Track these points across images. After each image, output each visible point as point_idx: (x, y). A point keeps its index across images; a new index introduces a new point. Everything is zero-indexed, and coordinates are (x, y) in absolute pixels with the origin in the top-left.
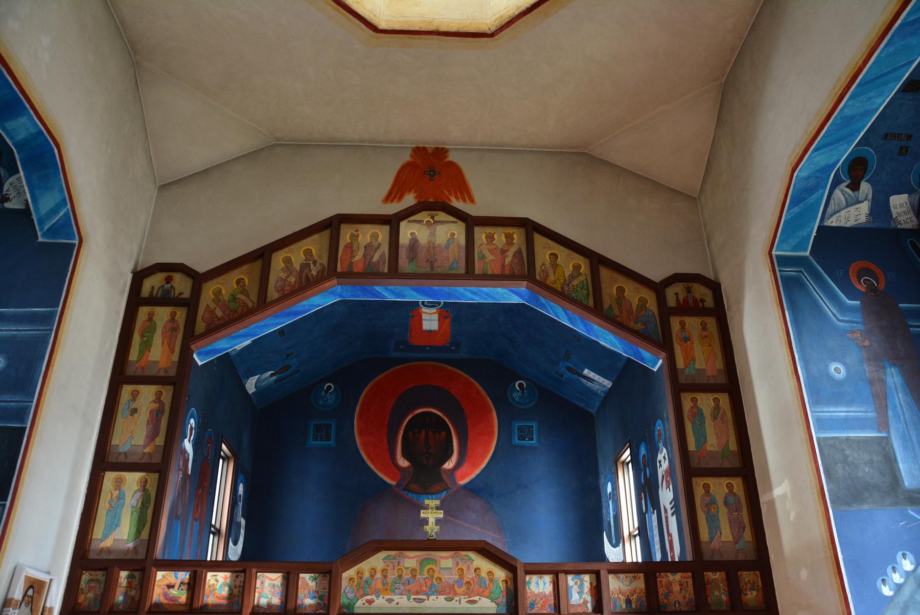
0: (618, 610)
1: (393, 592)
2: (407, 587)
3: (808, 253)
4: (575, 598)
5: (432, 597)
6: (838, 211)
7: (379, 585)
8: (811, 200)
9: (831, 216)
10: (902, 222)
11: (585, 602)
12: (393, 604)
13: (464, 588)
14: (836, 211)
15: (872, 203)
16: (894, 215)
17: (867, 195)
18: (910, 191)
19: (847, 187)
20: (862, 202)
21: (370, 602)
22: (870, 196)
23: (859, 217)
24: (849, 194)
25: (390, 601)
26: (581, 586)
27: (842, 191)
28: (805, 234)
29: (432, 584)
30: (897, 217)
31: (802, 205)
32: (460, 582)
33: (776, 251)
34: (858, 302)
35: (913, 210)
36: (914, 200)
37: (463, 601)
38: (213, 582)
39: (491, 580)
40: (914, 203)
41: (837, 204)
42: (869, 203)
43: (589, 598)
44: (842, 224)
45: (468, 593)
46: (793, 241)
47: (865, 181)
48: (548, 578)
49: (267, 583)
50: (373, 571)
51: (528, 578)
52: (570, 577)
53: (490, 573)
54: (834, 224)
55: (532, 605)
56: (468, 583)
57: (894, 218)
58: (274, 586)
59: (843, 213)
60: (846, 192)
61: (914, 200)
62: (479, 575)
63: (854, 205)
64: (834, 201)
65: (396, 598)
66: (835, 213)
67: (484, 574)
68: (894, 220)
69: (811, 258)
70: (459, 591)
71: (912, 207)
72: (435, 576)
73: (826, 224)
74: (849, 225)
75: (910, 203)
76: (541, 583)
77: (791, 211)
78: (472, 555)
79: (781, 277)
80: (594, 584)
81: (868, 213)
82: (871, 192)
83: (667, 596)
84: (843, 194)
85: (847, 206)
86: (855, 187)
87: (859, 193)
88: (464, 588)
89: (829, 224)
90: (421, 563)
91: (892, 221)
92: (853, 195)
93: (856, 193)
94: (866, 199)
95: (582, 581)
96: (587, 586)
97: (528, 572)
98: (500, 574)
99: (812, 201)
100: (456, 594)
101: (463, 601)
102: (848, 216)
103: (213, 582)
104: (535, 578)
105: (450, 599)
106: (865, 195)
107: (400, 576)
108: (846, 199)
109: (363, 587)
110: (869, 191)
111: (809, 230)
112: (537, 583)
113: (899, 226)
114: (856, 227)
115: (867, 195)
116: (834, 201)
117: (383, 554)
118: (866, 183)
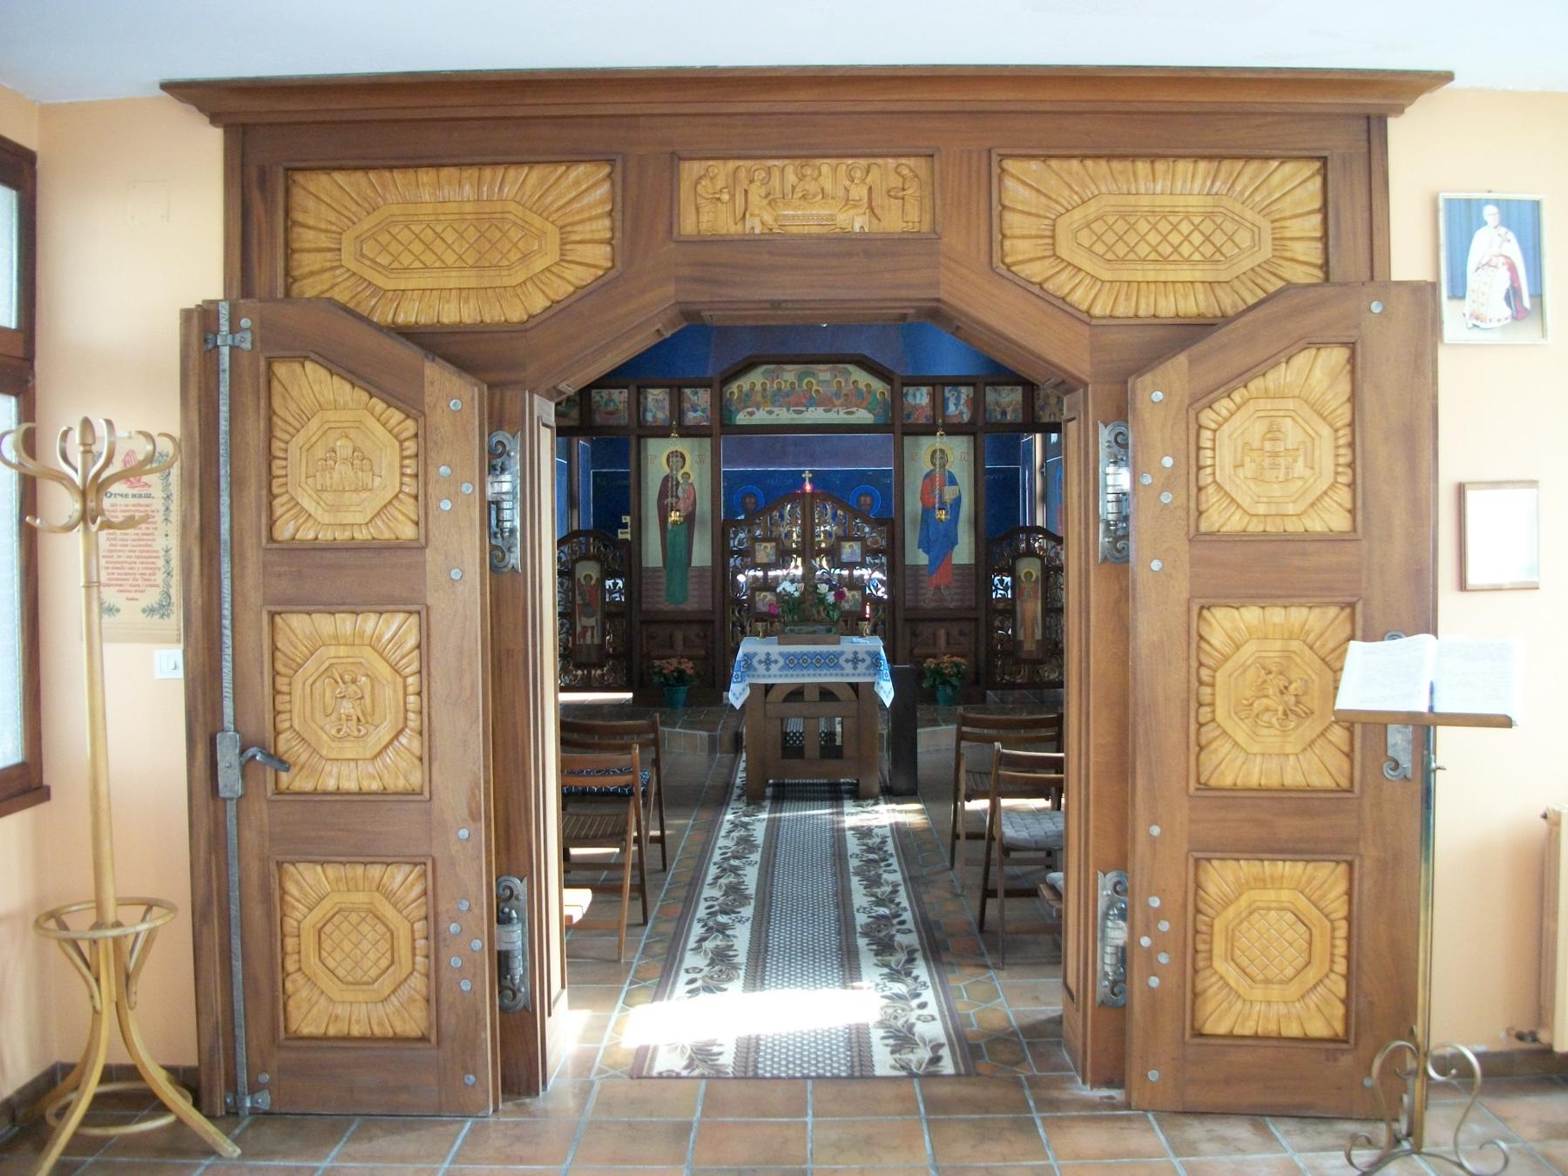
0: (993, 420)
1: (773, 404)
2: (787, 400)
4: (952, 408)
5: (811, 409)
7: (759, 398)
11: (961, 413)
12: (774, 416)
13: (842, 400)
21: (751, 414)
25: (770, 412)
26: (958, 399)
29: (811, 397)
32: (838, 395)
37: (841, 413)
38: (598, 398)
39: (869, 392)
43: (965, 410)
45: (847, 404)
48: (924, 390)
49: (650, 398)
50: (753, 385)
51: (905, 389)
52: (947, 389)
53: (868, 386)
55: (909, 417)
56: (846, 395)
58: (657, 401)
62: (856, 388)
65: (776, 410)
67: (862, 386)
70: (837, 402)
72: (814, 388)
76: (918, 395)
78: (850, 367)
80: (971, 395)
83: (1042, 408)
88: (842, 400)
90: (800, 377)
95: (959, 393)
96: (963, 397)
97: (904, 385)
98: (878, 386)
100: (834, 406)
101: (841, 413)
103: (598, 398)
104: (911, 390)
105: (829, 411)
107: (779, 389)
109: (747, 399)
112: (914, 395)
117: (765, 367)
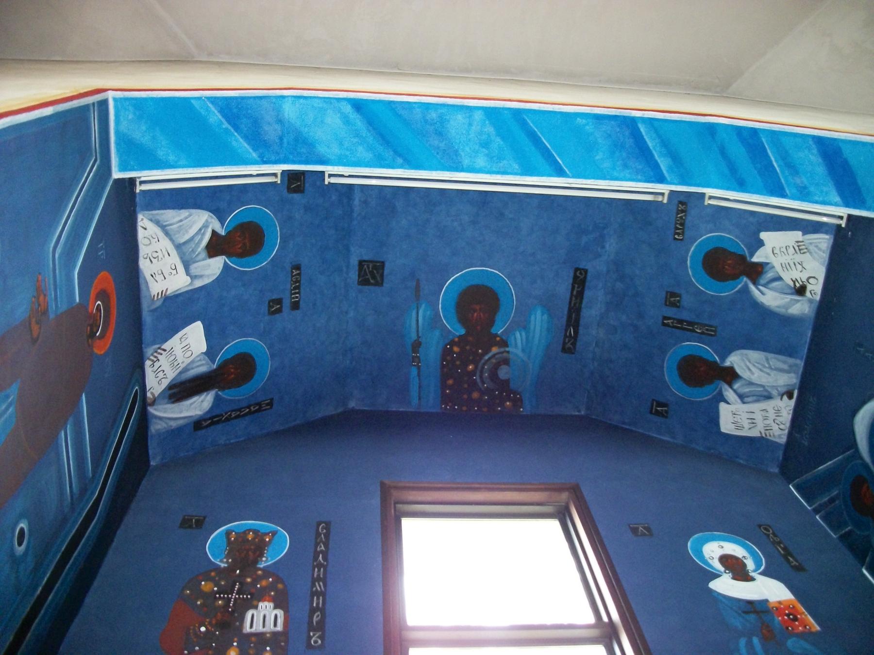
3: (117, 175)
6: (167, 234)
8: (237, 140)
9: (157, 223)
10: (157, 365)
14: (168, 228)
15: (187, 292)
16: (167, 346)
17: (201, 276)
18: (210, 353)
19: (214, 233)
20: (188, 273)
22: (198, 283)
23: (159, 278)
24: (201, 240)
27: (205, 226)
28: (161, 153)
30: (165, 350)
31: (226, 125)
33: (115, 99)
34: (78, 300)
35: (180, 373)
36: (198, 366)
40: (192, 369)
41: (180, 226)
42: (188, 286)
44: (143, 250)
46: (141, 134)
47: (225, 260)
54: (141, 234)
57: (162, 347)
59: (166, 244)
60: (204, 234)
61: (198, 366)
63: (181, 258)
64: (186, 218)
66: (163, 228)
68: (159, 348)
69: (111, 183)
71: (185, 370)
73: (140, 217)
74: (144, 265)
75: (193, 362)
77: (210, 105)
79: (86, 107)
81: (168, 293)
82: (206, 281)
84: (200, 230)
85: (178, 247)
86: (216, 247)
87: (203, 260)
89: (140, 224)
91: (158, 346)
92: (199, 249)
93: (204, 254)
94: (193, 278)
99: (234, 143)
102: (161, 256)
106: (199, 274)
108: (192, 239)
110: (208, 276)
111: (172, 158)
113: (148, 363)
114: (141, 281)
115: (201, 276)
116: (186, 218)
118: (221, 266)
